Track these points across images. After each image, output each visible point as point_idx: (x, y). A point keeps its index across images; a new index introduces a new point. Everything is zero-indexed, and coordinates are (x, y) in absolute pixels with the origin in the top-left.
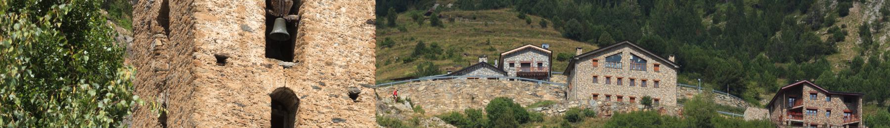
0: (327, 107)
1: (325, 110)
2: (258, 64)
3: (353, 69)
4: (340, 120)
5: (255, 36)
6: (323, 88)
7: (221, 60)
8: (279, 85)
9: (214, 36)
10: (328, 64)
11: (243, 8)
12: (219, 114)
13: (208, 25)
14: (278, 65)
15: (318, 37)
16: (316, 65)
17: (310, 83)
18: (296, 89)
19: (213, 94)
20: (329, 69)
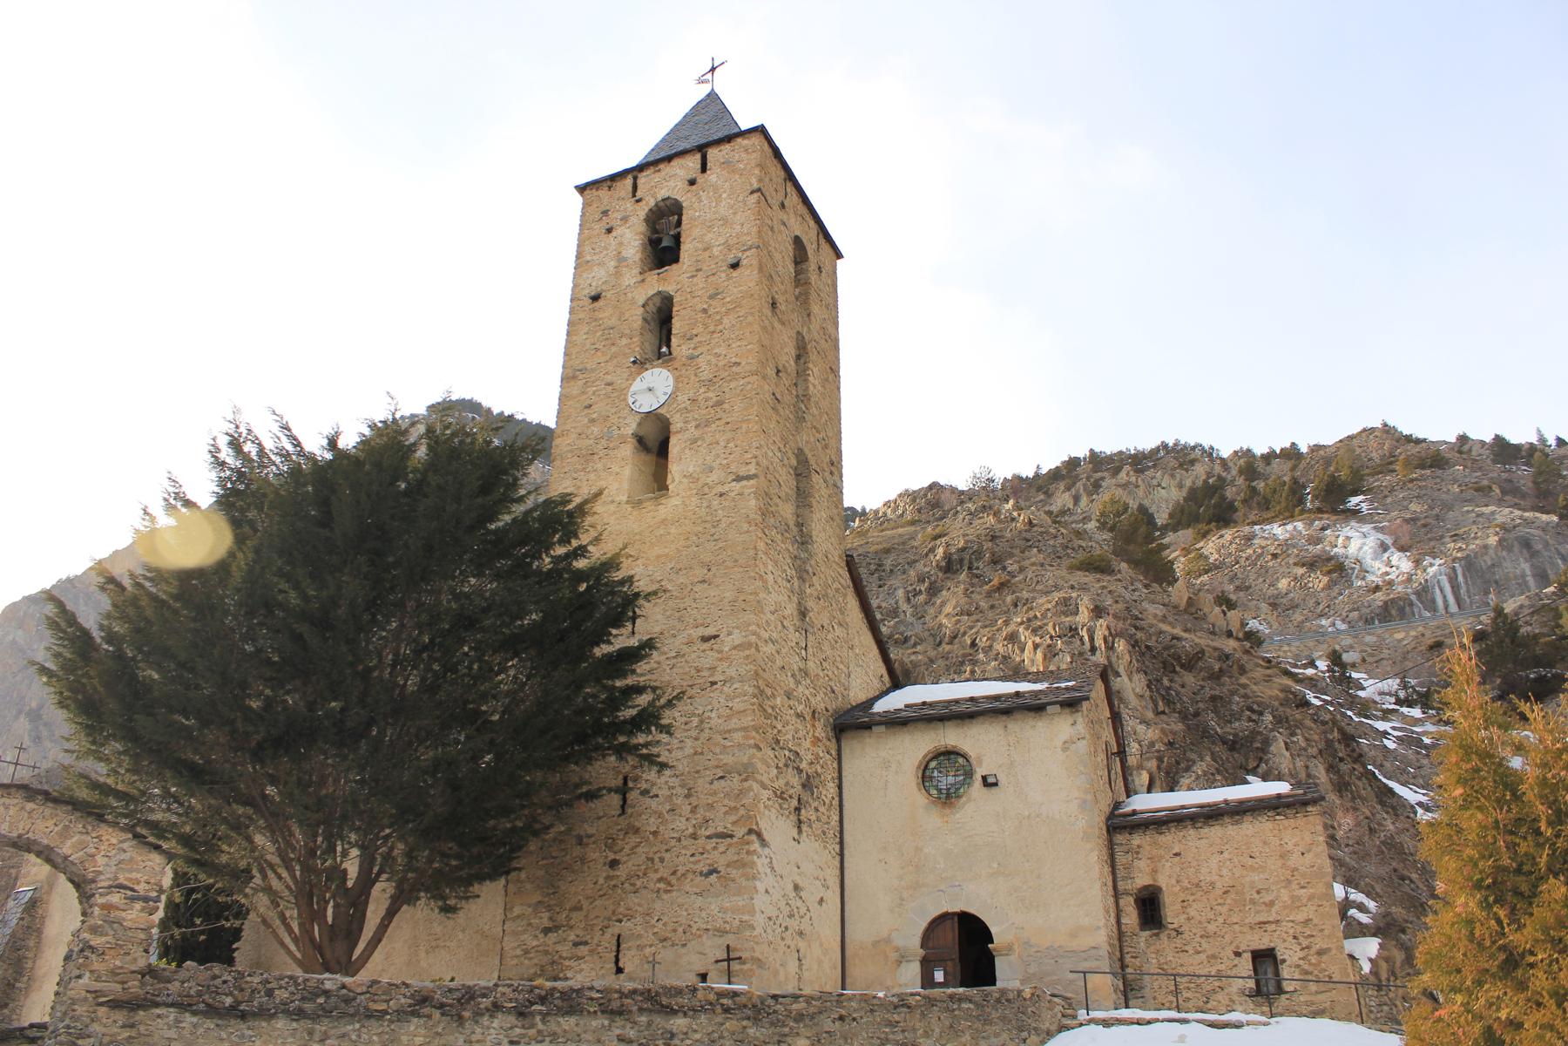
4: (717, 294)
5: (630, 261)
6: (701, 273)
7: (595, 298)
8: (651, 293)
9: (589, 282)
10: (705, 250)
11: (621, 244)
12: (588, 347)
14: (652, 277)
15: (696, 232)
18: (670, 288)
20: (707, 254)
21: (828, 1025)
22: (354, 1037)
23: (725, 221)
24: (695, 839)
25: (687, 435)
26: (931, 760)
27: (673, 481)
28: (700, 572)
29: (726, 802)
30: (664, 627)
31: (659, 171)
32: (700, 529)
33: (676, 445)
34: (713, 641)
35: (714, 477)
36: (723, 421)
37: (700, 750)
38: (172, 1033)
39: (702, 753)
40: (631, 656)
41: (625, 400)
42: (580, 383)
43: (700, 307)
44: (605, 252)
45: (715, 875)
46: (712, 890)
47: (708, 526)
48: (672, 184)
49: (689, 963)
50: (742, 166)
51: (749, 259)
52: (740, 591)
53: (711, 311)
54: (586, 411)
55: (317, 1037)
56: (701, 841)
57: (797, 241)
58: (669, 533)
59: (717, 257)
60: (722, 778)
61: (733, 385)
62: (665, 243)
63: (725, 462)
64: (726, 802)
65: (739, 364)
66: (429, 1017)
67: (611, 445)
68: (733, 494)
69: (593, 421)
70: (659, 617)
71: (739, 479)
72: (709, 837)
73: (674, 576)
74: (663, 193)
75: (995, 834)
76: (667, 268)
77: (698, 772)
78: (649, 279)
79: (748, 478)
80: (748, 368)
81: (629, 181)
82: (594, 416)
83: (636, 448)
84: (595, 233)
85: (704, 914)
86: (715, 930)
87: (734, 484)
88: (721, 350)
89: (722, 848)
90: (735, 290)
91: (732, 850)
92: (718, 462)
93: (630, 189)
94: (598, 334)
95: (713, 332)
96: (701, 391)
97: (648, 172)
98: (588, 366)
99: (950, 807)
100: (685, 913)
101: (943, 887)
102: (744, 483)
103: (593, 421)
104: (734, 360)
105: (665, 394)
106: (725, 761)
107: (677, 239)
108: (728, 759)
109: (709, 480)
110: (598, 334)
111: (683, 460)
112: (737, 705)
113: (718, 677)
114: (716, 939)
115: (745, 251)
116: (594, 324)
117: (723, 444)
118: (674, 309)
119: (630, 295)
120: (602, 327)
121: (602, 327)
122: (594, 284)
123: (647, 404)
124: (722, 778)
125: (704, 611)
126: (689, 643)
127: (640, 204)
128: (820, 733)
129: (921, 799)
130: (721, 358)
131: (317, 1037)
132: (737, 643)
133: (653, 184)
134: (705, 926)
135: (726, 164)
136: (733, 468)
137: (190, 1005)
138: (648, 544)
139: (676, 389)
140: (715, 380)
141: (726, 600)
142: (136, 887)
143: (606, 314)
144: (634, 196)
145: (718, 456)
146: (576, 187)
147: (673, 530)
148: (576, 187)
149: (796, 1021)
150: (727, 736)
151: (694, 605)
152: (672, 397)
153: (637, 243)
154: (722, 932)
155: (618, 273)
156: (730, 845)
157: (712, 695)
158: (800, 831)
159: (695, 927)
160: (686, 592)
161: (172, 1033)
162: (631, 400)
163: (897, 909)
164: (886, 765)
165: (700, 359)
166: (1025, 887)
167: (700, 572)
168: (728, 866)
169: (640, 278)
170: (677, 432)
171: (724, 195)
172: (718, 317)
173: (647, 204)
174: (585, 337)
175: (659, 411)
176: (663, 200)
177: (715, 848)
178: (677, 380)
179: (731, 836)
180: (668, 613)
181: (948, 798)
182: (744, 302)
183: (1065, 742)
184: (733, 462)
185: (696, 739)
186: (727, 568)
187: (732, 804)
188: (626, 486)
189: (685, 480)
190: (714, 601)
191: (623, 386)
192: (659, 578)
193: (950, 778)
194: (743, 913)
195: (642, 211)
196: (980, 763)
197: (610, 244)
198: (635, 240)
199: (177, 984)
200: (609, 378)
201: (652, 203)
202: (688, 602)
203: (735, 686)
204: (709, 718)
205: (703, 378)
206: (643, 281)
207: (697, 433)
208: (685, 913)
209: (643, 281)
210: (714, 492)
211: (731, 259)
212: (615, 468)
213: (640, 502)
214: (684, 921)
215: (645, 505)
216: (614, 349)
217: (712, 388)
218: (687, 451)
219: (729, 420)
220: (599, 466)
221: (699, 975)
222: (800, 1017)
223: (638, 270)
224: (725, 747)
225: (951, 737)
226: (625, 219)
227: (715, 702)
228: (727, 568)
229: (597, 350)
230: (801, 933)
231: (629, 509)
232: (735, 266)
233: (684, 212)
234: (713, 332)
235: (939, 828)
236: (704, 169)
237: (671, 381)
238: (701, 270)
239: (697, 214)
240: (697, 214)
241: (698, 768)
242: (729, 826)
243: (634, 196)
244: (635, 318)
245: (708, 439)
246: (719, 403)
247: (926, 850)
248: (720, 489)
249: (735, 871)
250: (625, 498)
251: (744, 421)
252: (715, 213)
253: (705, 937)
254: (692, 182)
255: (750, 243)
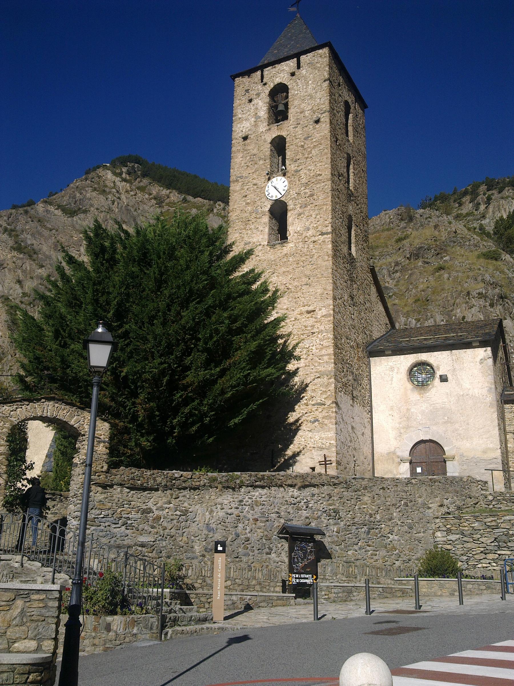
0: (301, 134)
1: (299, 136)
2: (264, 131)
3: (315, 109)
4: (308, 137)
5: (262, 118)
8: (274, 136)
9: (241, 129)
10: (301, 113)
11: (257, 109)
12: (243, 165)
13: (239, 125)
14: (274, 127)
15: (296, 103)
16: (295, 116)
17: (291, 127)
18: (284, 134)
19: (239, 157)
20: (302, 115)
21: (378, 492)
22: (188, 497)
23: (311, 97)
24: (307, 405)
25: (296, 212)
26: (415, 367)
27: (290, 234)
28: (305, 280)
29: (321, 388)
30: (288, 306)
31: (275, 67)
32: (304, 259)
33: (290, 217)
34: (312, 313)
35: (310, 233)
36: (314, 205)
37: (308, 364)
38: (120, 496)
39: (309, 366)
40: (277, 322)
41: (264, 193)
42: (240, 184)
43: (299, 144)
44: (249, 113)
45: (317, 422)
46: (316, 429)
47: (308, 257)
48: (282, 75)
49: (306, 463)
50: (319, 66)
51: (325, 118)
52: (325, 289)
53: (306, 146)
54: (244, 199)
55: (174, 497)
56: (310, 407)
57: (346, 103)
58: (289, 261)
59: (308, 117)
60: (319, 377)
61: (318, 186)
62: (281, 107)
63: (315, 225)
64: (321, 388)
65: (321, 175)
66: (217, 488)
67: (258, 216)
68: (320, 242)
69: (248, 204)
70: (286, 301)
71: (322, 234)
72: (313, 405)
73: (292, 282)
74: (277, 80)
75: (446, 403)
76: (281, 122)
77: (307, 375)
78: (273, 128)
79: (327, 233)
80: (325, 177)
81: (259, 73)
82: (248, 201)
83: (270, 217)
84: (243, 102)
85: (312, 441)
86: (318, 447)
87: (320, 236)
88: (312, 167)
89: (320, 410)
90: (318, 135)
91: (325, 411)
92: (312, 225)
93: (259, 77)
94: (248, 158)
95: (307, 158)
96: (302, 189)
97: (269, 68)
98: (244, 175)
99: (423, 390)
100: (303, 440)
101: (421, 428)
102: (325, 236)
103: (248, 204)
104: (318, 172)
105: (284, 190)
106: (320, 370)
107: (286, 105)
108: (321, 369)
109: (308, 234)
110: (248, 158)
111: (295, 224)
112: (325, 343)
113: (315, 330)
114: (318, 452)
115: (322, 113)
116: (245, 152)
117: (314, 216)
118: (287, 145)
119: (263, 137)
120: (250, 154)
121: (250, 154)
122: (244, 130)
123: (275, 195)
124: (319, 377)
125: (308, 299)
126: (301, 314)
127: (266, 86)
128: (361, 354)
129: (409, 386)
130: (312, 172)
131: (174, 497)
132: (324, 314)
133: (272, 75)
134: (313, 446)
135: (311, 64)
136: (320, 228)
137: (125, 484)
138: (279, 266)
139: (290, 188)
140: (309, 183)
141: (318, 294)
142: (100, 437)
143: (252, 147)
144: (262, 82)
145: (312, 222)
146: (231, 76)
147: (291, 259)
148: (231, 76)
149: (363, 489)
150: (321, 358)
151: (302, 296)
152: (288, 192)
153: (265, 108)
154: (321, 449)
155: (256, 125)
156: (324, 408)
157: (313, 338)
158: (353, 402)
159: (308, 446)
160: (298, 289)
161: (120, 496)
162: (267, 193)
163: (398, 438)
164: (392, 369)
165: (301, 172)
166: (461, 429)
167: (305, 280)
168: (323, 418)
169: (267, 128)
170: (291, 210)
171: (310, 82)
172: (309, 150)
173: (269, 86)
174: (241, 159)
175: (281, 199)
176: (278, 84)
177: (317, 410)
178: (290, 182)
179: (324, 405)
180: (290, 299)
181: (422, 385)
182: (323, 141)
183: (481, 360)
184: (319, 225)
185: (306, 359)
186: (318, 278)
187: (324, 390)
188: (266, 237)
189: (296, 234)
190: (312, 293)
191: (262, 186)
192: (285, 283)
193: (423, 376)
194: (331, 440)
195: (267, 90)
196: (438, 369)
197: (251, 109)
198: (264, 106)
199: (119, 476)
200: (255, 181)
201: (272, 86)
202: (299, 294)
203: (324, 334)
204: (312, 349)
205: (303, 182)
206: (270, 129)
207: (301, 211)
208: (303, 440)
209: (270, 129)
210: (310, 240)
211: (315, 118)
212: (261, 228)
213: (274, 245)
214: (303, 443)
215: (276, 246)
216: (256, 166)
217: (307, 188)
218: (296, 220)
219: (316, 204)
220: (252, 227)
221: (311, 468)
222: (365, 488)
223: (266, 124)
224: (320, 363)
225: (424, 357)
226: (258, 95)
227: (314, 342)
228: (318, 278)
229: (248, 166)
230: (355, 449)
231: (269, 249)
232: (317, 122)
233: (289, 91)
234: (307, 158)
235: (418, 400)
236: (299, 67)
237: (286, 183)
238: (299, 124)
239: (296, 92)
240: (296, 92)
241: (307, 373)
242: (323, 400)
243: (262, 82)
244: (267, 149)
245: (307, 214)
246: (312, 195)
247: (412, 410)
248: (313, 239)
249: (326, 421)
250: (266, 243)
251: (324, 205)
252: (306, 92)
253: (313, 450)
254: (293, 74)
255: (325, 109)
